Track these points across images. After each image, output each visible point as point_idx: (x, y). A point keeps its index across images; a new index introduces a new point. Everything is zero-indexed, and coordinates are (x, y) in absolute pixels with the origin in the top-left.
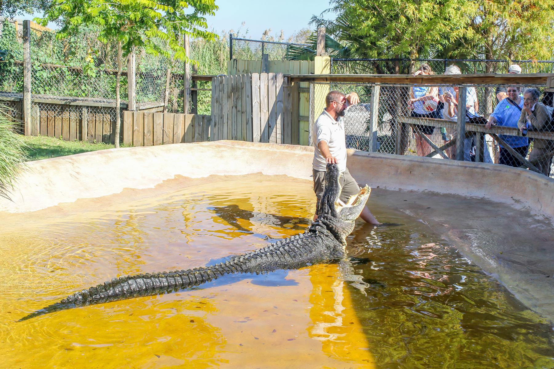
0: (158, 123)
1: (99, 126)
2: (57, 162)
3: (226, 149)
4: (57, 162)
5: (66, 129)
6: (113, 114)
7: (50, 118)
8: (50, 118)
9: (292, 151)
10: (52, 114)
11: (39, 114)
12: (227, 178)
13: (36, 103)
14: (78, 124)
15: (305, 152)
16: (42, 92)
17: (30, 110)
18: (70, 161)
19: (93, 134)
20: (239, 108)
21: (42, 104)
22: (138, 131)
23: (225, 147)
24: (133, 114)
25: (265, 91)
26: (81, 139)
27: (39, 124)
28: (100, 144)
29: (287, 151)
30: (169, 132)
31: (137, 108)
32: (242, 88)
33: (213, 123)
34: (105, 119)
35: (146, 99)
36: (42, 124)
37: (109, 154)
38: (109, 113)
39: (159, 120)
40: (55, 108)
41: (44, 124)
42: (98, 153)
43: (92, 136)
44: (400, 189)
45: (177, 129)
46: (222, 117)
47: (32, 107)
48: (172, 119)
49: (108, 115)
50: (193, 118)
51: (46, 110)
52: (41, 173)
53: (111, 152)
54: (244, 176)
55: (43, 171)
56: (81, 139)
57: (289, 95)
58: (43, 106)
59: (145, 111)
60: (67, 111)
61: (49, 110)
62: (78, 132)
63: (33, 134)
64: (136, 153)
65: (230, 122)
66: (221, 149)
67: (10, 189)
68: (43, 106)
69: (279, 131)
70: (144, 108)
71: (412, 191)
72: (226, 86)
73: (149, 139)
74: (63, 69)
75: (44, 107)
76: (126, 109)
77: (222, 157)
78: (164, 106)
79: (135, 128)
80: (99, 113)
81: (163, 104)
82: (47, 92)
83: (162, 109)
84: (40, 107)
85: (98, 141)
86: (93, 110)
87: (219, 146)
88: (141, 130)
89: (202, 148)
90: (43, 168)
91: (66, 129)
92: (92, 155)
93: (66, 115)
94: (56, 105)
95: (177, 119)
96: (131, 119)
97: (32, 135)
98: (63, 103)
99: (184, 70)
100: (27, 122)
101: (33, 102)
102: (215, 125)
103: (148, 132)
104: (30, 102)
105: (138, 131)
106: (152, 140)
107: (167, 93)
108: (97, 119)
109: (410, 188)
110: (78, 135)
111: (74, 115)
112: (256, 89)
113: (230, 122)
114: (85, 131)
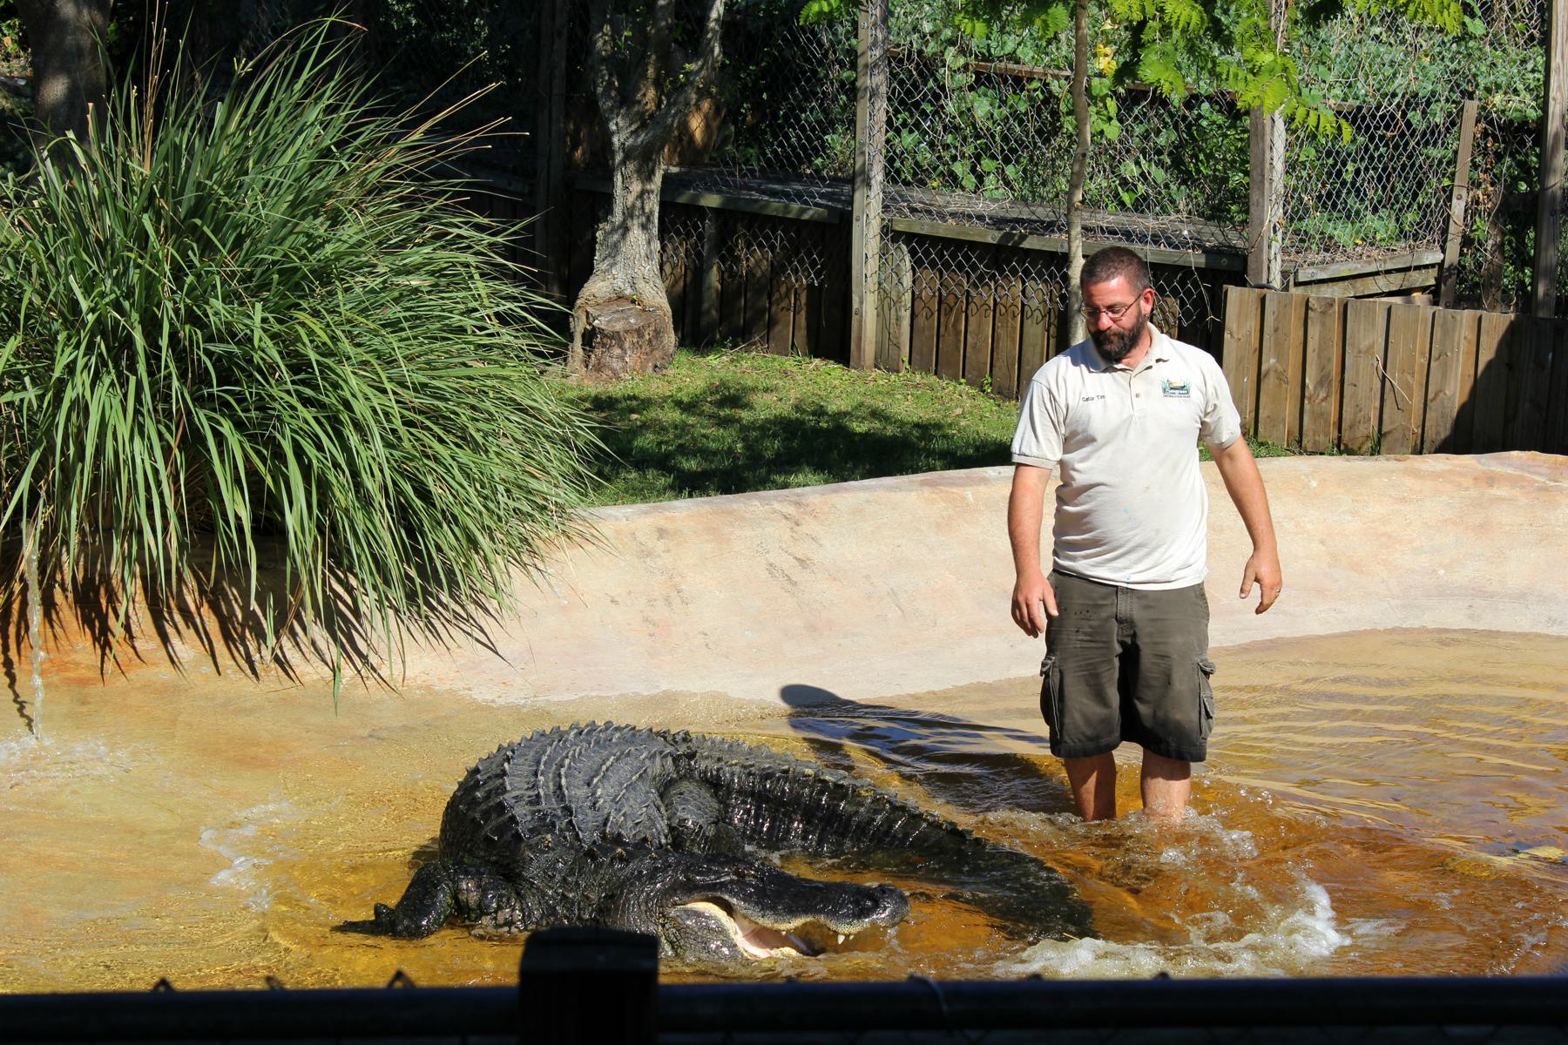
0: (1364, 345)
3: (1516, 492)
4: (731, 513)
6: (1188, 294)
7: (951, 300)
8: (951, 300)
11: (907, 280)
14: (1053, 330)
16: (970, 181)
17: (873, 264)
18: (791, 510)
21: (922, 239)
23: (1514, 481)
24: (1263, 300)
27: (906, 323)
30: (1409, 388)
31: (1285, 274)
35: (1342, 232)
36: (921, 321)
37: (969, 493)
38: (1175, 293)
39: (1367, 335)
40: (968, 259)
41: (928, 324)
42: (924, 483)
45: (1444, 376)
47: (884, 252)
48: (1423, 331)
49: (1171, 300)
50: (1513, 328)
51: (933, 264)
53: (984, 481)
55: (660, 546)
59: (1313, 293)
60: (1014, 272)
61: (947, 266)
63: (885, 362)
66: (1496, 491)
73: (1320, 416)
74: (1055, 87)
75: (927, 253)
76: (1242, 283)
77: (1483, 528)
78: (1441, 265)
79: (1270, 362)
81: (1434, 257)
82: (990, 181)
84: (913, 252)
88: (1293, 373)
89: (1409, 482)
94: (973, 245)
95: (1445, 333)
96: (1253, 323)
98: (992, 237)
99: (1544, 107)
101: (886, 230)
103: (1323, 381)
104: (875, 226)
105: (1281, 377)
106: (1333, 417)
107: (1458, 208)
111: (1037, 293)
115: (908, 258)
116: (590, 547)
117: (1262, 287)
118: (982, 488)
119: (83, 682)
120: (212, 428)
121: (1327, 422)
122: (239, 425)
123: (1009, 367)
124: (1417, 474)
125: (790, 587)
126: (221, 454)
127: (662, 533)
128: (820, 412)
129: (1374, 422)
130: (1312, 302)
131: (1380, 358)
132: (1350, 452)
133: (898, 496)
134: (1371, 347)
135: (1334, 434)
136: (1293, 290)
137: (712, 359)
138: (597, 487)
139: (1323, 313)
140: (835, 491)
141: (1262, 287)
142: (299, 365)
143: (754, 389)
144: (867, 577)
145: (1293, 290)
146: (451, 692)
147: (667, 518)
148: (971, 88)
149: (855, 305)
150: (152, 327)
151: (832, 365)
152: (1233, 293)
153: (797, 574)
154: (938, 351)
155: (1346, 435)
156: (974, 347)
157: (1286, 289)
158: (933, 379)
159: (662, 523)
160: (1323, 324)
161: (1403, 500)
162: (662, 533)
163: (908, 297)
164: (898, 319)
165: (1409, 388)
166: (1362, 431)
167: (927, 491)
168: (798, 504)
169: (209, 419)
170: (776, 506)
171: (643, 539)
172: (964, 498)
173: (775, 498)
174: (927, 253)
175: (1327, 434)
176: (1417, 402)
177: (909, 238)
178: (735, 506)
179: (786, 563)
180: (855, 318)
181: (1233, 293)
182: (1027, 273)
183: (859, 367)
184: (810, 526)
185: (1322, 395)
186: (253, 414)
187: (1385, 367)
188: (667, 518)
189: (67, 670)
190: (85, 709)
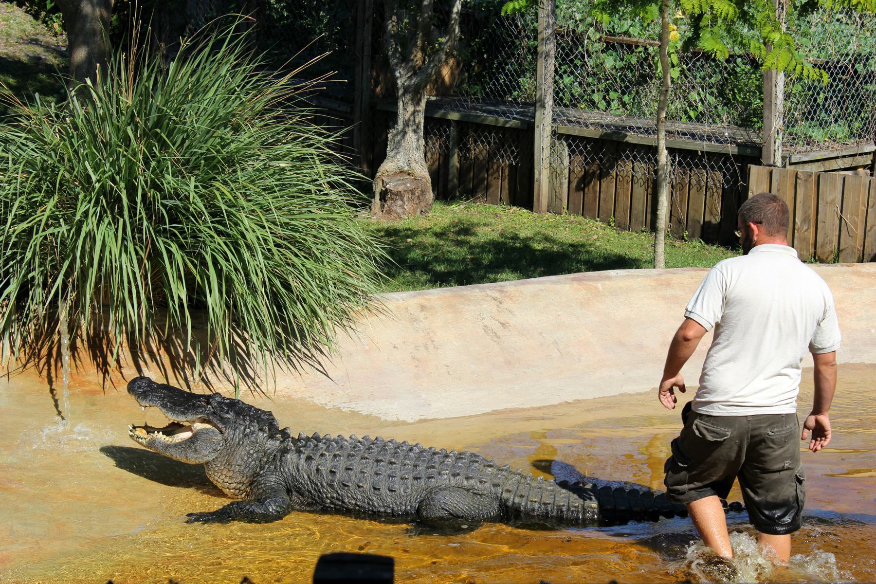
0: (829, 199)
2: (463, 296)
4: (463, 296)
5: (624, 201)
6: (728, 169)
11: (566, 161)
13: (560, 137)
14: (650, 190)
16: (602, 105)
17: (547, 152)
18: (497, 295)
19: (683, 216)
24: (771, 173)
27: (565, 186)
28: (698, 243)
30: (855, 224)
31: (784, 158)
34: (711, 183)
35: (817, 134)
37: (599, 285)
38: (720, 169)
39: (831, 193)
42: (573, 279)
43: (679, 221)
47: (553, 145)
48: (864, 191)
51: (581, 153)
52: (413, 320)
53: (608, 278)
55: (422, 315)
56: (654, 228)
59: (800, 169)
60: (627, 157)
62: (649, 210)
63: (554, 209)
64: (668, 284)
70: (807, 159)
75: (577, 146)
76: (758, 163)
80: (697, 166)
82: (615, 104)
84: (569, 146)
85: (692, 236)
86: (684, 158)
89: (855, 278)
91: (624, 201)
92: (558, 282)
97: (548, 211)
100: (539, 181)
101: (554, 133)
103: (805, 220)
104: (548, 130)
106: (812, 241)
108: (694, 182)
110: (649, 216)
111: (641, 169)
115: (566, 149)
116: (381, 316)
117: (770, 166)
118: (607, 282)
119: (93, 393)
120: (166, 248)
121: (808, 243)
122: (181, 247)
123: (625, 212)
124: (858, 274)
125: (496, 339)
126: (171, 263)
127: (423, 308)
128: (515, 238)
129: (835, 243)
130: (799, 174)
131: (839, 206)
132: (822, 261)
133: (558, 287)
134: (834, 200)
135: (812, 250)
136: (788, 167)
137: (454, 207)
138: (386, 282)
139: (806, 181)
140: (523, 284)
141: (770, 166)
142: (215, 212)
143: (478, 225)
144: (541, 333)
145: (788, 167)
146: (302, 399)
147: (426, 300)
148: (603, 52)
149: (536, 176)
150: (132, 191)
151: (523, 210)
152: (754, 169)
153: (500, 331)
155: (818, 253)
156: (605, 200)
157: (784, 167)
158: (581, 218)
159: (423, 302)
160: (806, 187)
161: (851, 289)
162: (423, 308)
163: (567, 171)
164: (561, 184)
165: (855, 224)
166: (828, 248)
167: (575, 284)
168: (501, 291)
169: (165, 243)
170: (489, 292)
171: (412, 312)
172: (597, 288)
173: (488, 288)
174: (577, 146)
175: (808, 251)
176: (860, 232)
177: (567, 137)
178: (465, 293)
179: (495, 325)
180: (536, 183)
181: (754, 169)
182: (635, 157)
183: (539, 211)
184: (508, 304)
185: (805, 228)
186: (189, 240)
187: (841, 212)
188: (426, 300)
189: (84, 386)
190: (93, 408)
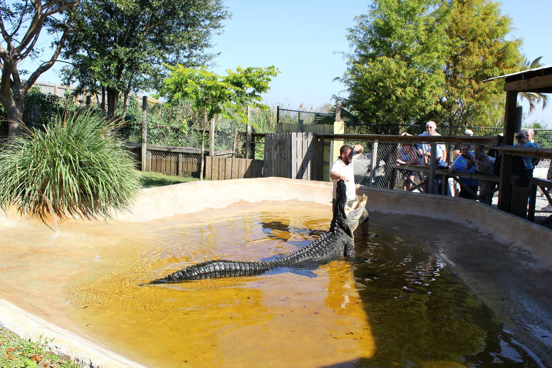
1: (190, 166)
5: (168, 167)
9: (318, 186)
10: (159, 157)
11: (151, 157)
12: (274, 203)
13: (149, 150)
15: (326, 186)
16: (153, 143)
20: (283, 156)
21: (153, 151)
22: (215, 170)
25: (300, 145)
26: (177, 174)
28: (191, 178)
29: (314, 185)
32: (285, 142)
33: (265, 165)
35: (221, 149)
39: (229, 162)
41: (154, 164)
44: (391, 213)
46: (271, 162)
50: (252, 162)
54: (285, 201)
56: (177, 174)
57: (316, 147)
58: (155, 152)
63: (147, 170)
65: (276, 165)
67: (132, 206)
68: (155, 152)
69: (309, 172)
71: (398, 214)
72: (274, 141)
76: (208, 155)
79: (214, 167)
81: (232, 152)
83: (231, 155)
85: (189, 176)
87: (269, 181)
90: (153, 193)
91: (168, 167)
93: (169, 158)
94: (162, 151)
96: (211, 162)
98: (166, 150)
99: (247, 129)
102: (266, 167)
103: (222, 170)
105: (215, 170)
107: (235, 145)
109: (398, 212)
111: (173, 158)
112: (294, 143)
113: (276, 165)
114: (180, 169)
122: (89, 174)
150: (74, 156)
154: (156, 168)
176: (237, 173)
177: (151, 150)
